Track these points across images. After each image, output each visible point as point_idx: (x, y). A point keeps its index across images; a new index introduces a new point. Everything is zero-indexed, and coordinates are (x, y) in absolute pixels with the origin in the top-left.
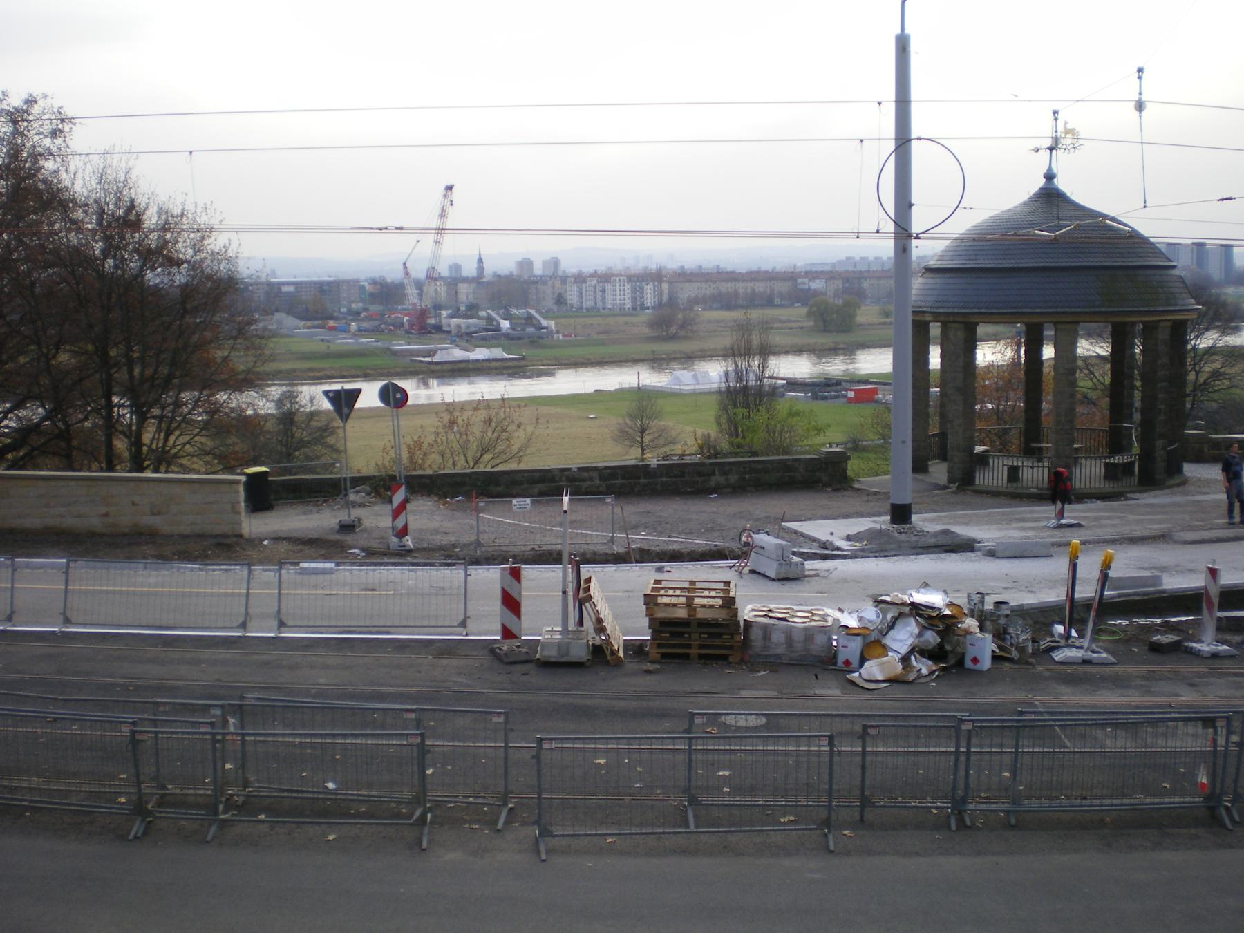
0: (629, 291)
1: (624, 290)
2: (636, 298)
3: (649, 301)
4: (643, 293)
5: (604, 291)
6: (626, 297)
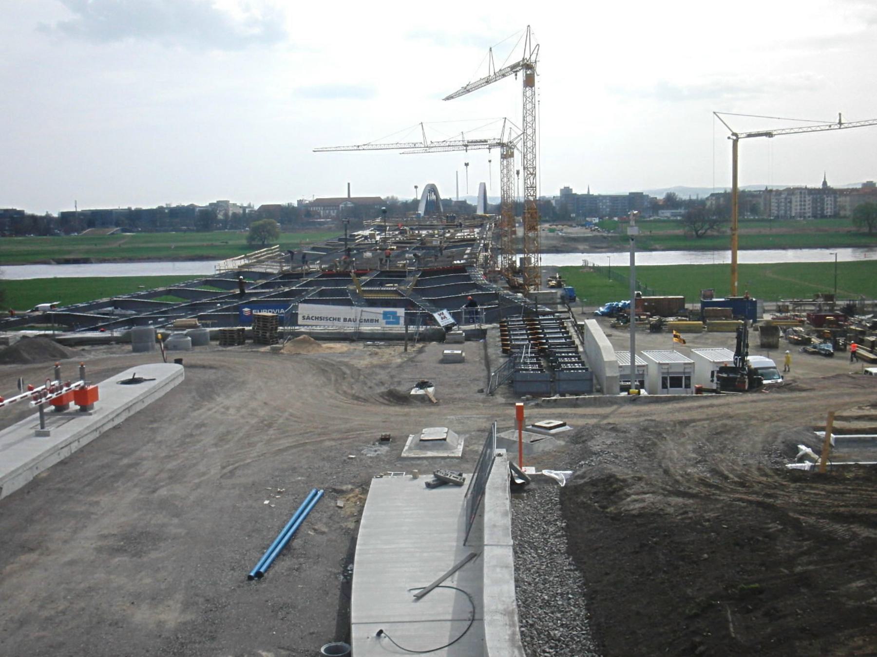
0: (810, 202)
1: (805, 201)
2: (816, 208)
3: (829, 210)
4: (823, 204)
5: (790, 202)
6: (807, 207)
